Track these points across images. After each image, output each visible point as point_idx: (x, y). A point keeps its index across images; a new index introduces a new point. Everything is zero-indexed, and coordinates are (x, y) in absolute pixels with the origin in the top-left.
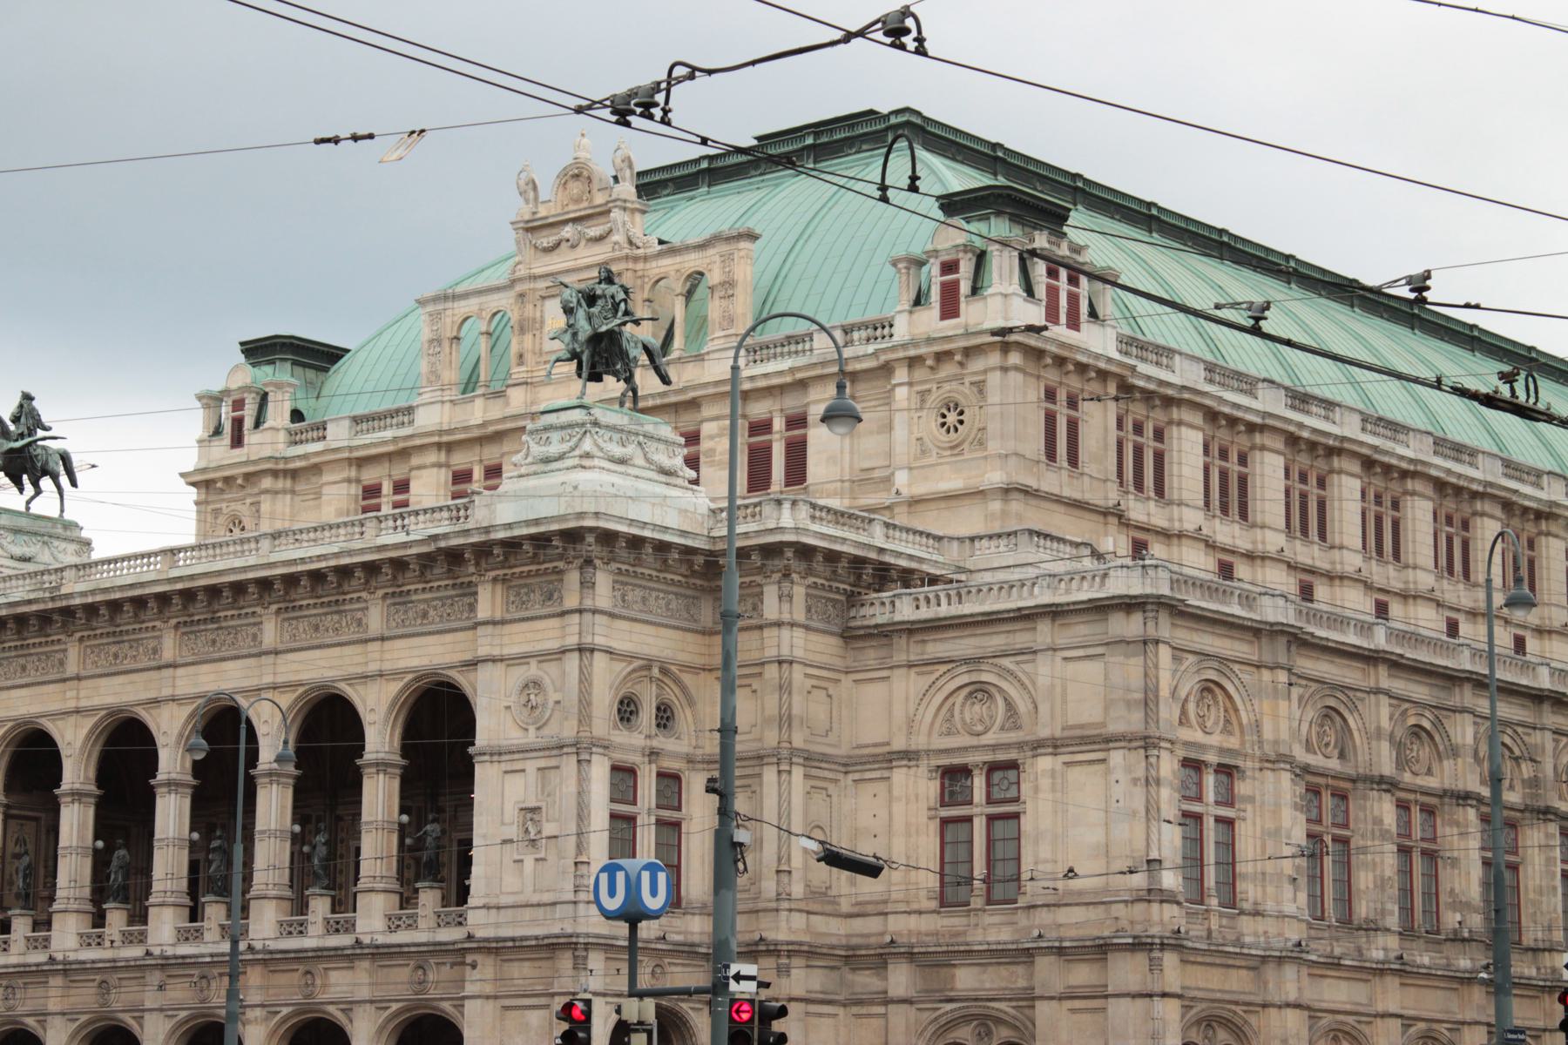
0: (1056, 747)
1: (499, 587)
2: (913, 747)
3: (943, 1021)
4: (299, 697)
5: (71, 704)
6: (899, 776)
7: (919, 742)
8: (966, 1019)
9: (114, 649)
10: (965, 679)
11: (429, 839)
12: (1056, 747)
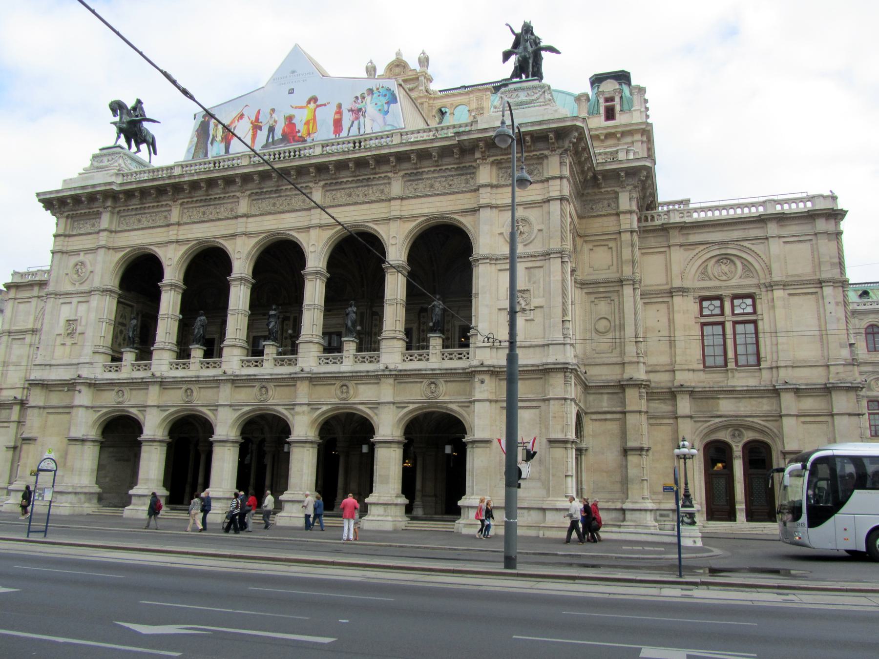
0: (784, 285)
1: (494, 169)
2: (685, 286)
3: (712, 427)
4: (335, 233)
5: (173, 238)
6: (677, 300)
7: (687, 284)
8: (725, 427)
9: (202, 209)
10: (717, 252)
11: (437, 309)
12: (784, 285)
